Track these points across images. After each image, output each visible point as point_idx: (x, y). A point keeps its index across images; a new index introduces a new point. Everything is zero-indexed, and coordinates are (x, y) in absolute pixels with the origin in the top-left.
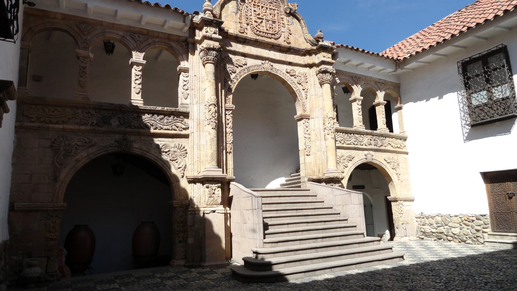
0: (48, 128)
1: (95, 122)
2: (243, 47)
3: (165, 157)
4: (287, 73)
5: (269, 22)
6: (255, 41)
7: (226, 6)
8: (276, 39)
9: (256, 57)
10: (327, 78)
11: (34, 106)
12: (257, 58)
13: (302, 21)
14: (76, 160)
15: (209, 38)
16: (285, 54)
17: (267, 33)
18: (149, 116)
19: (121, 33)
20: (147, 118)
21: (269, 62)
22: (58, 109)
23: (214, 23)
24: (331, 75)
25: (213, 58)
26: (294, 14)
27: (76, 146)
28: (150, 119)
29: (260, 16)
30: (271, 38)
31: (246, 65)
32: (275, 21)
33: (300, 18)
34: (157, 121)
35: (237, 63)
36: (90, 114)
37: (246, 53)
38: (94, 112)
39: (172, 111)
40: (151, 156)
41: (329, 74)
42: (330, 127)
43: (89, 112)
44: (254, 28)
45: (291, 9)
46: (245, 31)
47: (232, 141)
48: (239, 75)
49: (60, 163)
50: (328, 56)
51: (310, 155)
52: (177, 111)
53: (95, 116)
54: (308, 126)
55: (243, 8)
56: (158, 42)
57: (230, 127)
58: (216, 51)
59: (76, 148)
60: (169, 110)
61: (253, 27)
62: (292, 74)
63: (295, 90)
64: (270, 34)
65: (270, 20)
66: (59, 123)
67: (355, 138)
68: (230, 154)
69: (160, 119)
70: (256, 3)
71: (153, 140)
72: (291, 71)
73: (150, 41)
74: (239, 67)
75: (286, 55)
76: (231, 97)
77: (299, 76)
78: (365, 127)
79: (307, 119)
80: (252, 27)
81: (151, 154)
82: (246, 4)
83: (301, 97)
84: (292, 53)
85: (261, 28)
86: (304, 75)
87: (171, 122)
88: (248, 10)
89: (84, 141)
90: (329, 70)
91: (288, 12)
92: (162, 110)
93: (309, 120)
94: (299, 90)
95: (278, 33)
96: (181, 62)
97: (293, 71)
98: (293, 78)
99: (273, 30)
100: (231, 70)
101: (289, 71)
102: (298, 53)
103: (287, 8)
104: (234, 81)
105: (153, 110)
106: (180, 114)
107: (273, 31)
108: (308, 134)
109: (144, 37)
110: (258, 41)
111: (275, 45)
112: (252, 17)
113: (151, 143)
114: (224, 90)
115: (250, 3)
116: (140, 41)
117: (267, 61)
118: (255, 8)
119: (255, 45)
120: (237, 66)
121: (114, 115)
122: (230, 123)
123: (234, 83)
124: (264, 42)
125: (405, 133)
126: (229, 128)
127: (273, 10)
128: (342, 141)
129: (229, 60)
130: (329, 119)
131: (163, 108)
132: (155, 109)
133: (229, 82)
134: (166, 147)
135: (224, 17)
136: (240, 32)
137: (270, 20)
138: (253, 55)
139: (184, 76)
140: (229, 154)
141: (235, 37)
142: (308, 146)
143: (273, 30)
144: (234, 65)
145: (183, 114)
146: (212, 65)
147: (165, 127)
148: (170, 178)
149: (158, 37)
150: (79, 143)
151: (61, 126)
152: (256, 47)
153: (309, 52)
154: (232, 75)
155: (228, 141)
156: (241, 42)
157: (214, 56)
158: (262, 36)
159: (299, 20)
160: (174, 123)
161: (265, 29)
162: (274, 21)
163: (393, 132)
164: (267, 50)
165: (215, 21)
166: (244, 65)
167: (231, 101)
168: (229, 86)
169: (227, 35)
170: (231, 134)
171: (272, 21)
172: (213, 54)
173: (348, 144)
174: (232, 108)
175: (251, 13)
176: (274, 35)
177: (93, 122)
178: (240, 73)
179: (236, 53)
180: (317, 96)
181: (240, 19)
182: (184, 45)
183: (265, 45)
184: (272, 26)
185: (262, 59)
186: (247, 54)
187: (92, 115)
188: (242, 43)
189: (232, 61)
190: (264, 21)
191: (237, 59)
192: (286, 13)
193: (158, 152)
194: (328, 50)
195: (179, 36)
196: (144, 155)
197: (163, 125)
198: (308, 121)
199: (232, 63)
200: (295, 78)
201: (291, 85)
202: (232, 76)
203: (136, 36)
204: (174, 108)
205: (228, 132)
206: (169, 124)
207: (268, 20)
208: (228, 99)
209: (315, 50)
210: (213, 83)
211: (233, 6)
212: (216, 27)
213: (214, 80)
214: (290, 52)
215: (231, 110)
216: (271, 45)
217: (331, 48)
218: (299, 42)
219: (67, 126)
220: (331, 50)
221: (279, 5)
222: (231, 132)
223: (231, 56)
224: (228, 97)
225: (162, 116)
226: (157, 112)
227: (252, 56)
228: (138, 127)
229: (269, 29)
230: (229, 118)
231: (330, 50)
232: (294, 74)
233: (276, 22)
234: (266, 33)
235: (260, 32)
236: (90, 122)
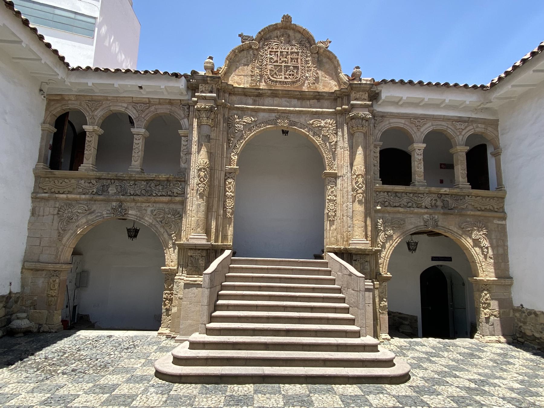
0: (56, 198)
1: (95, 191)
11: (47, 179)
14: (77, 226)
19: (125, 105)
22: (66, 180)
27: (77, 213)
32: (297, 65)
34: (153, 188)
36: (91, 184)
38: (95, 181)
43: (91, 182)
44: (269, 78)
49: (62, 229)
53: (95, 186)
59: (77, 215)
61: (267, 77)
63: (318, 144)
66: (65, 193)
67: (408, 198)
78: (426, 184)
80: (266, 77)
86: (333, 124)
88: (262, 60)
89: (84, 209)
107: (293, 78)
109: (145, 105)
115: (266, 50)
116: (142, 110)
118: (272, 55)
121: (112, 183)
123: (240, 143)
125: (503, 189)
128: (386, 202)
139: (184, 141)
150: (79, 211)
151: (64, 196)
155: (228, 206)
161: (283, 77)
163: (488, 189)
167: (235, 163)
171: (293, 66)
173: (396, 206)
175: (267, 62)
177: (94, 191)
181: (252, 71)
182: (186, 109)
187: (93, 184)
203: (138, 105)
219: (70, 196)
228: (134, 194)
229: (287, 77)
230: (232, 181)
236: (91, 191)
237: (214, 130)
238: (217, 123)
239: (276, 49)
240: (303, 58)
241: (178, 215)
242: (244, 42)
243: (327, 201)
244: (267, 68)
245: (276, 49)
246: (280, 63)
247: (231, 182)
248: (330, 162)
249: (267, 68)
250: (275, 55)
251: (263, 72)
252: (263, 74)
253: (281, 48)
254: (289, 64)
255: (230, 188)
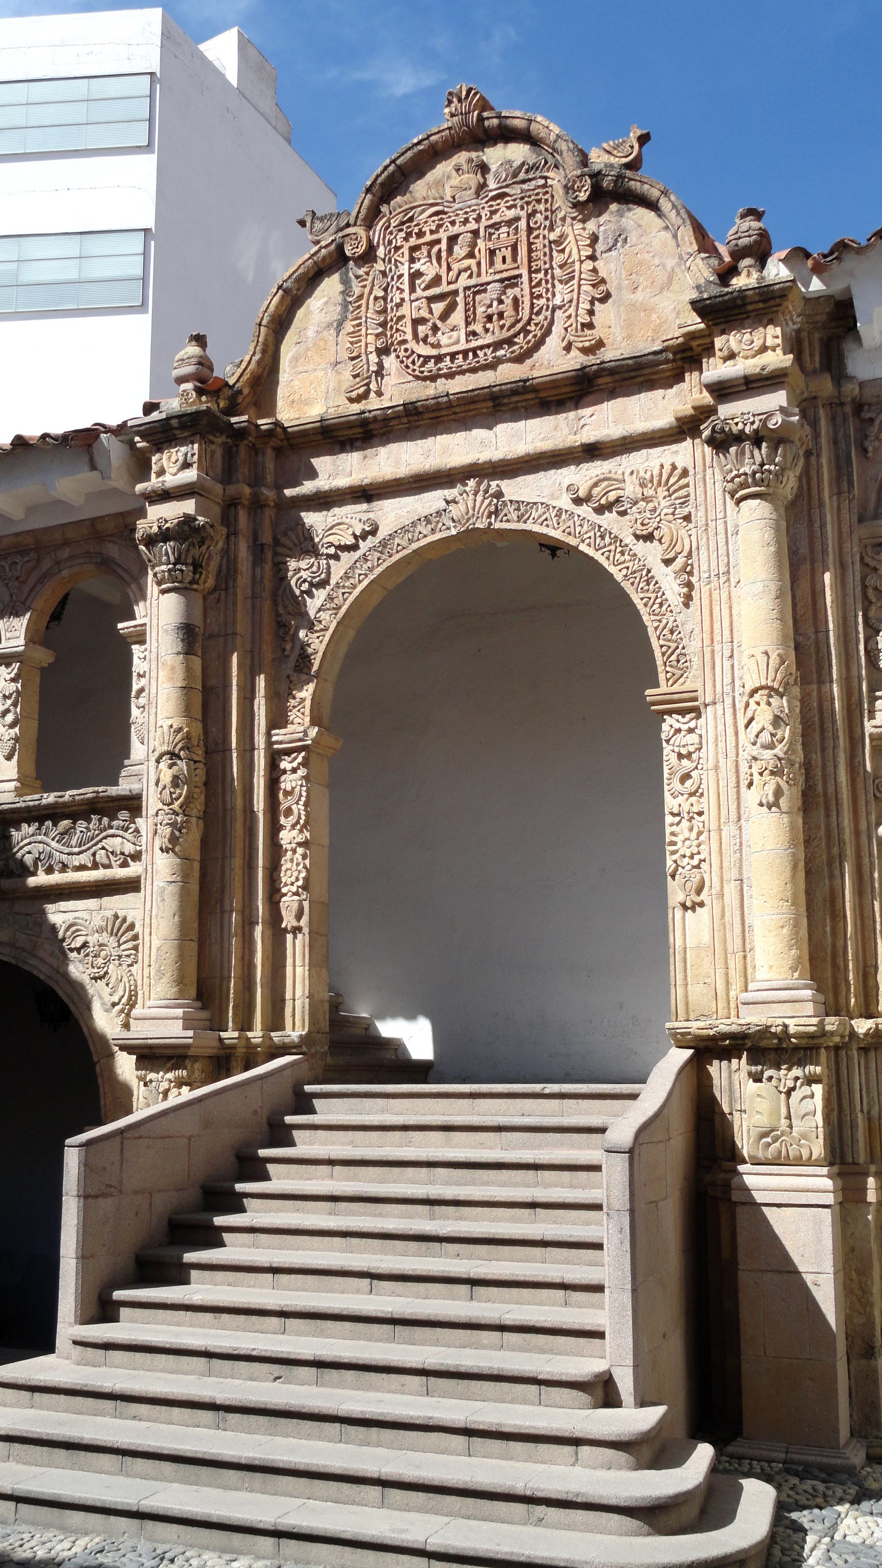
2: (365, 457)
3: (77, 970)
4: (578, 501)
5: (485, 291)
6: (406, 416)
7: (300, 313)
8: (519, 359)
9: (415, 482)
10: (741, 472)
12: (424, 483)
13: (665, 205)
15: (159, 495)
16: (572, 415)
17: (474, 351)
18: (32, 829)
20: (26, 838)
21: (479, 484)
23: (177, 428)
24: (760, 449)
25: (169, 570)
26: (621, 190)
28: (32, 839)
29: (444, 288)
30: (492, 366)
31: (373, 532)
32: (516, 272)
33: (655, 193)
35: (331, 539)
37: (366, 481)
39: (88, 799)
40: (42, 972)
41: (747, 445)
42: (754, 744)
45: (596, 176)
46: (371, 386)
47: (300, 883)
48: (344, 587)
50: (757, 344)
51: (702, 904)
52: (103, 797)
54: (692, 749)
55: (365, 286)
56: (71, 558)
57: (298, 822)
58: (174, 539)
60: (77, 798)
62: (603, 501)
63: (619, 577)
64: (488, 346)
65: (488, 283)
68: (299, 936)
69: (62, 834)
70: (428, 233)
71: (43, 913)
72: (596, 485)
73: (46, 564)
74: (344, 556)
75: (579, 411)
76: (307, 693)
77: (643, 500)
79: (683, 712)
81: (42, 960)
82: (379, 266)
83: (655, 607)
84: (613, 394)
85: (444, 340)
86: (672, 481)
87: (92, 839)
90: (740, 426)
91: (583, 196)
92: (56, 803)
93: (699, 716)
94: (644, 573)
95: (528, 323)
96: (136, 608)
97: (606, 483)
98: (608, 520)
99: (501, 323)
100: (305, 581)
101: (582, 493)
102: (641, 379)
103: (574, 182)
104: (320, 622)
105: (34, 806)
106: (116, 804)
108: (691, 795)
110: (416, 408)
111: (501, 391)
112: (405, 310)
113: (40, 920)
114: (262, 676)
115: (397, 249)
116: (18, 578)
117: (472, 483)
119: (417, 427)
120: (332, 551)
122: (294, 807)
123: (322, 630)
124: (445, 399)
126: (293, 827)
127: (504, 229)
129: (296, 541)
130: (752, 701)
131: (59, 794)
132: (37, 803)
133: (302, 634)
134: (77, 930)
135: (287, 364)
136: (351, 400)
137: (488, 283)
138: (396, 480)
140: (295, 937)
141: (322, 433)
142: (686, 860)
143: (501, 323)
144: (316, 554)
145: (125, 803)
146: (173, 596)
147: (76, 861)
148: (90, 1041)
149: (66, 543)
152: (424, 436)
153: (688, 354)
154: (316, 597)
155: (286, 885)
156: (357, 439)
157: (172, 559)
158: (450, 376)
159: (652, 205)
160: (100, 841)
162: (509, 279)
164: (476, 432)
165: (174, 422)
166: (364, 536)
167: (307, 711)
168: (302, 648)
169: (288, 439)
170: (300, 850)
171: (501, 281)
172: (167, 554)
174: (300, 740)
176: (510, 342)
178: (348, 578)
179: (329, 500)
180: (722, 579)
183: (457, 410)
184: (501, 302)
185: (447, 480)
186: (371, 484)
188: (358, 444)
189: (312, 539)
190: (460, 299)
191: (331, 521)
192: (576, 205)
193: (57, 951)
194: (750, 308)
195: (121, 514)
196: (20, 965)
197: (69, 854)
198: (692, 724)
199: (311, 550)
200: (623, 513)
201: (602, 560)
202: (312, 605)
204: (91, 789)
205: (289, 847)
206: (83, 848)
207: (482, 285)
208: (294, 707)
209: (704, 336)
210: (173, 668)
211: (326, 299)
212: (192, 439)
213: (178, 653)
214: (602, 390)
215: (298, 750)
216: (485, 400)
217: (760, 294)
218: (654, 317)
220: (772, 303)
221: (541, 182)
222: (300, 844)
223: (310, 518)
224: (294, 698)
225: (65, 823)
226: (50, 811)
227: (398, 485)
229: (478, 327)
231: (761, 305)
232: (612, 496)
233: (520, 276)
234: (465, 353)
235: (439, 359)
237: (219, 600)
238: (228, 569)
239: (432, 232)
240: (537, 237)
241: (129, 935)
242: (318, 242)
243: (669, 819)
244: (403, 317)
245: (432, 232)
246: (449, 283)
247: (293, 788)
248: (673, 645)
249: (403, 317)
250: (429, 256)
251: (392, 336)
252: (392, 343)
253: (453, 223)
254: (484, 279)
255: (289, 812)
